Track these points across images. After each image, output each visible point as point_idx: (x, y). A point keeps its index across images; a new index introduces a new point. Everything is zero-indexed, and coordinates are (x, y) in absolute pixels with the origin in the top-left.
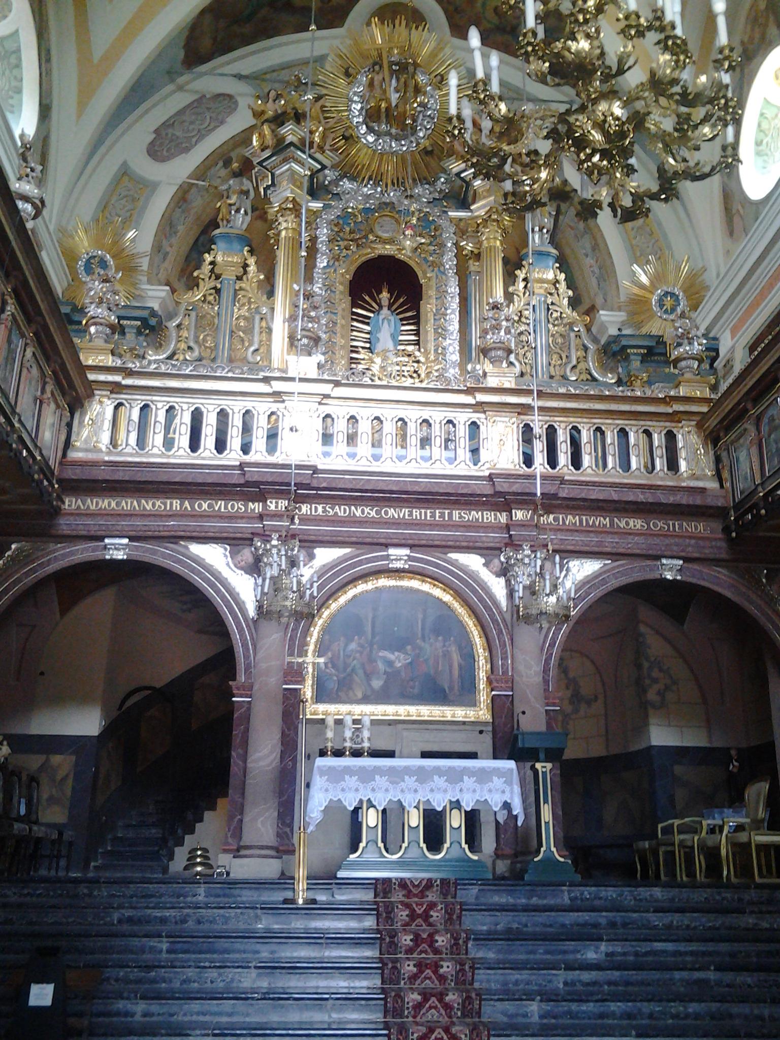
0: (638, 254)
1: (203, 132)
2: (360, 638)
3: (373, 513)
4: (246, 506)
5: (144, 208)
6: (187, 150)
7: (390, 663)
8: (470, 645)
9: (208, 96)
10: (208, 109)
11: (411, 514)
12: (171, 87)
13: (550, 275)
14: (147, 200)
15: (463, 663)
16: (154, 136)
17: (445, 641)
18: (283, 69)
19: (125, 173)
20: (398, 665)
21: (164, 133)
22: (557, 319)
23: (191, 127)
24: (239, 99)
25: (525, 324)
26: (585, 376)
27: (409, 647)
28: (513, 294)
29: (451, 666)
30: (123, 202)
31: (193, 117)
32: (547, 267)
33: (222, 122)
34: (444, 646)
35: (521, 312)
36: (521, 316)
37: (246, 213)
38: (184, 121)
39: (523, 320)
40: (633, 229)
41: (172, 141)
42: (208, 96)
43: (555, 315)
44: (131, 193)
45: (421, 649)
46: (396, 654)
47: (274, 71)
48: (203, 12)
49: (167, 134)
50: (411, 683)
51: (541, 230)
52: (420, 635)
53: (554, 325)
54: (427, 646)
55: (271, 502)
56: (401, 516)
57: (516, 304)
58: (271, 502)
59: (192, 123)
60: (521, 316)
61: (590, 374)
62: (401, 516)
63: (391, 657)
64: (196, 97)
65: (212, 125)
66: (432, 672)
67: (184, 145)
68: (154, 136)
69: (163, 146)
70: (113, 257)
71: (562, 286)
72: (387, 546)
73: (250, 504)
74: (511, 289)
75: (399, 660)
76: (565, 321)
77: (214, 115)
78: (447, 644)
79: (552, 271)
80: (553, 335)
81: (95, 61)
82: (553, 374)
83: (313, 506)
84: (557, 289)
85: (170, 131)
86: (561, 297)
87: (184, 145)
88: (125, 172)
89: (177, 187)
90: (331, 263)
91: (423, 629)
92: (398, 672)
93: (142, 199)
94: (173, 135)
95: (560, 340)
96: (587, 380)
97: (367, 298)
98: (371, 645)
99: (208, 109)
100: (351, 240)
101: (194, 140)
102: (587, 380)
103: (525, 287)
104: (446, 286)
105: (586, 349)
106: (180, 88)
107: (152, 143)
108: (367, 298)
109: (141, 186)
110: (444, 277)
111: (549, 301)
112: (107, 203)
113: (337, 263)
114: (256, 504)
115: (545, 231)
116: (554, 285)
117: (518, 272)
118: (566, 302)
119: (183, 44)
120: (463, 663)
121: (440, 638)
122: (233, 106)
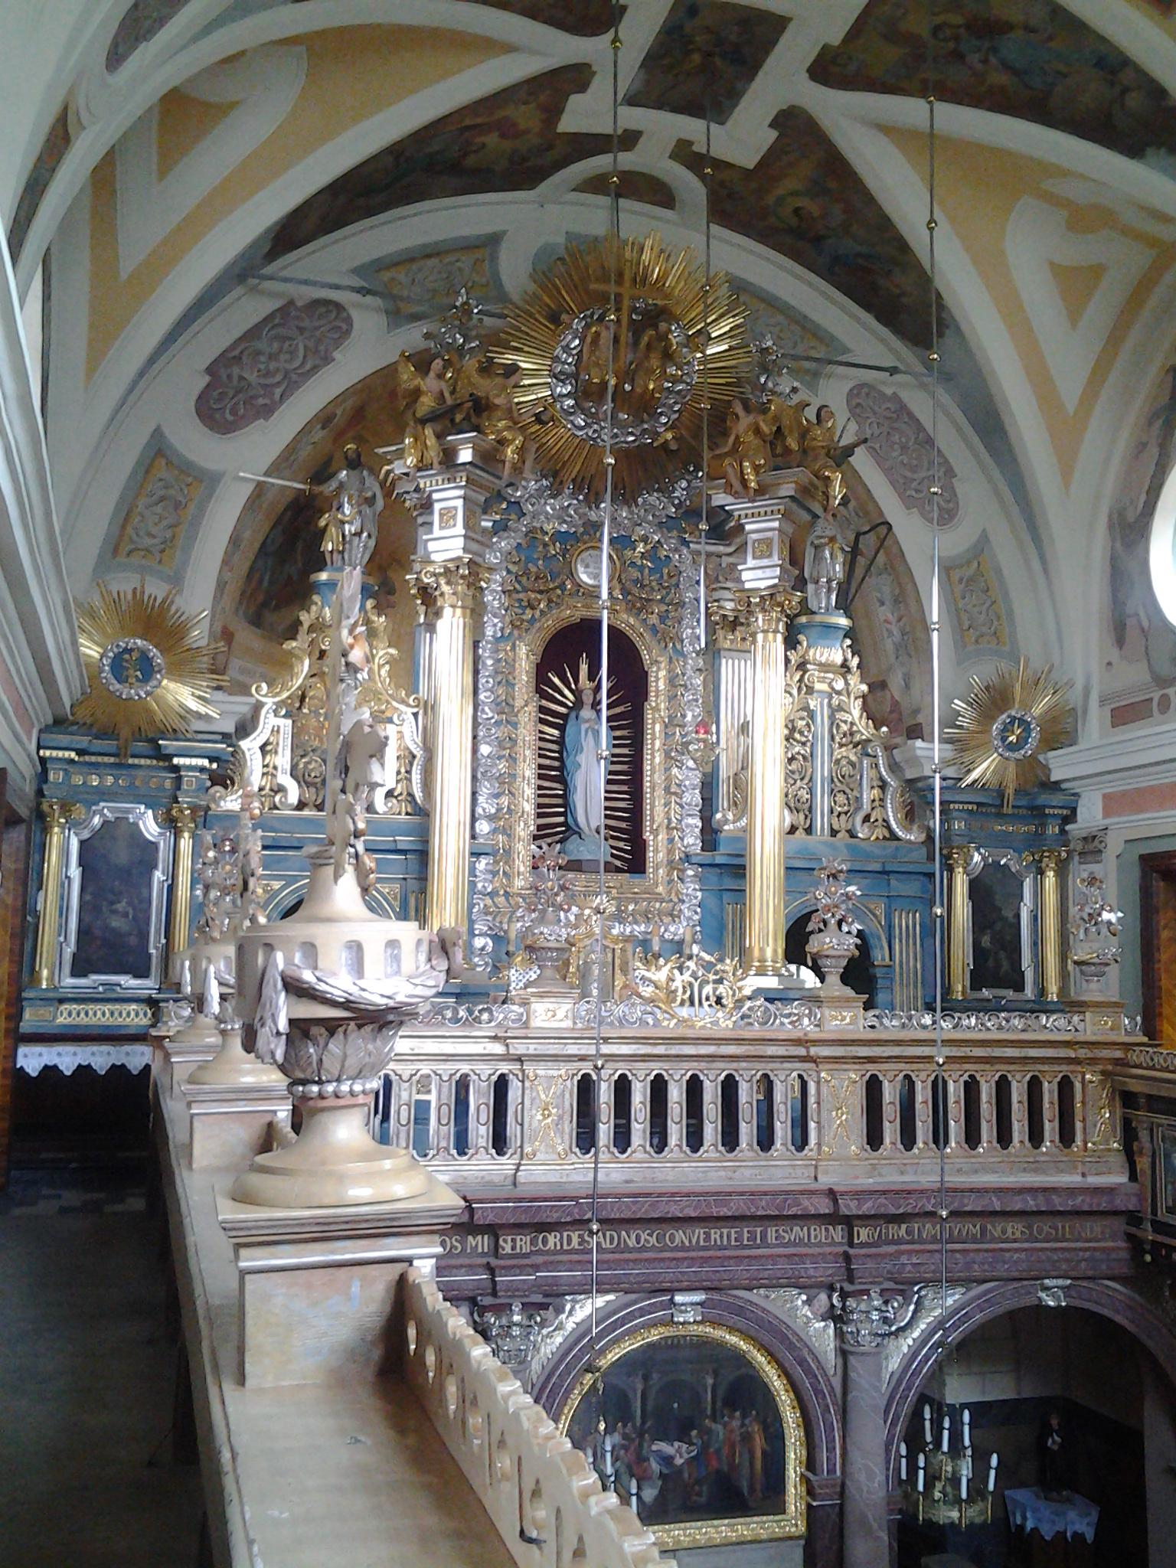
0: (966, 624)
1: (294, 377)
2: (625, 1426)
3: (653, 1240)
4: (463, 1242)
5: (196, 523)
6: (267, 411)
7: (667, 1460)
8: (779, 1419)
9: (299, 304)
10: (301, 330)
11: (708, 1236)
12: (239, 290)
15: (767, 1448)
16: (207, 378)
17: (744, 1416)
18: (428, 256)
20: (679, 1461)
21: (223, 373)
23: (273, 365)
24: (354, 314)
25: (798, 742)
26: (880, 832)
27: (694, 1433)
29: (752, 1453)
30: (159, 509)
31: (276, 345)
33: (327, 360)
34: (743, 1425)
35: (792, 721)
37: (369, 536)
38: (259, 353)
40: (961, 580)
41: (238, 392)
42: (299, 304)
43: (845, 728)
44: (172, 492)
45: (709, 1431)
46: (676, 1444)
47: (412, 260)
49: (229, 377)
50: (697, 1488)
51: (829, 581)
52: (709, 1412)
53: (841, 745)
54: (718, 1428)
55: (505, 1241)
56: (694, 1241)
58: (505, 1241)
59: (272, 357)
61: (889, 827)
62: (694, 1241)
63: (667, 1448)
64: (278, 304)
65: (308, 366)
66: (726, 1468)
67: (261, 401)
68: (207, 378)
69: (226, 402)
72: (672, 1291)
73: (470, 1238)
75: (679, 1452)
76: (857, 738)
77: (311, 344)
78: (747, 1422)
79: (840, 652)
82: (836, 827)
83: (565, 1234)
85: (236, 371)
88: (158, 451)
91: (714, 1402)
92: (679, 1471)
93: (192, 508)
94: (241, 378)
96: (884, 838)
97: (556, 680)
98: (641, 1436)
99: (301, 330)
100: (541, 592)
101: (278, 391)
102: (884, 838)
105: (883, 786)
107: (202, 399)
108: (556, 680)
109: (190, 480)
113: (516, 632)
114: (479, 1237)
120: (767, 1448)
121: (738, 1414)
122: (344, 327)
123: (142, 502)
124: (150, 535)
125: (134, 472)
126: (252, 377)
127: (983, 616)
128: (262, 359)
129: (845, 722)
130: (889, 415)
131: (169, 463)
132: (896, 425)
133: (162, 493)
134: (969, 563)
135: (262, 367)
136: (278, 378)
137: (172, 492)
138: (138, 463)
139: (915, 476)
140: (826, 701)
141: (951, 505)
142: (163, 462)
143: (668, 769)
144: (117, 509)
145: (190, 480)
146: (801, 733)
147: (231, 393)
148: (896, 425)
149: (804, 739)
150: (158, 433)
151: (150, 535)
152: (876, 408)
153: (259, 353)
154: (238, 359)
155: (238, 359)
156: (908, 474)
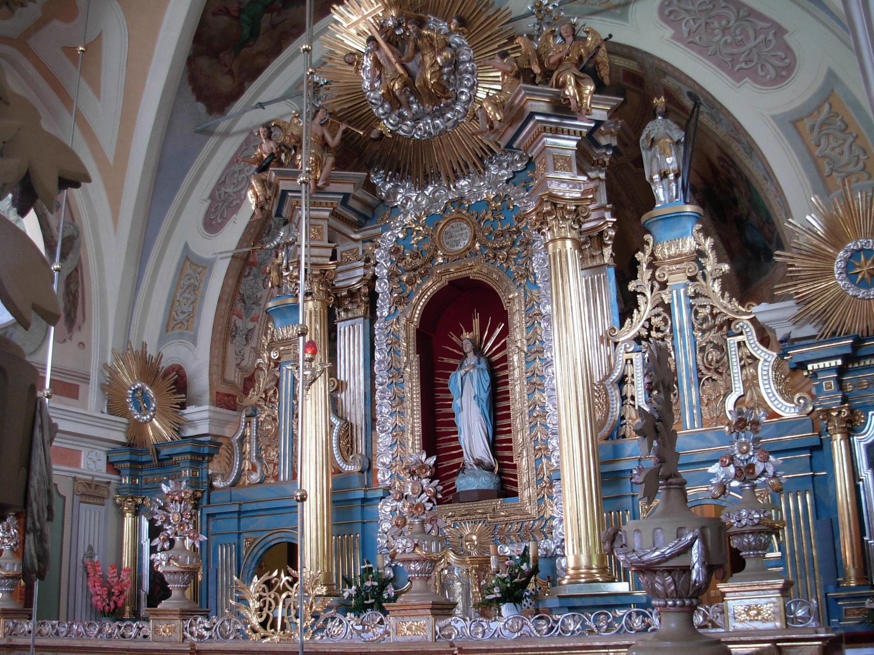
0: (827, 170)
5: (203, 297)
13: (689, 244)
14: (206, 286)
16: (209, 201)
19: (187, 258)
22: (705, 319)
28: (635, 293)
30: (186, 295)
32: (683, 236)
36: (650, 329)
38: (235, 172)
39: (653, 334)
40: (812, 128)
48: (190, 61)
51: (664, 176)
53: (704, 332)
57: (642, 308)
60: (650, 329)
64: (242, 138)
67: (235, 203)
70: (150, 387)
71: (710, 263)
74: (631, 286)
76: (719, 320)
80: (702, 349)
81: (111, 161)
84: (702, 268)
86: (709, 278)
87: (235, 203)
89: (229, 260)
90: (393, 309)
94: (225, 193)
95: (714, 355)
103: (653, 278)
104: (538, 305)
106: (226, 134)
110: (535, 291)
111: (691, 291)
112: (173, 301)
115: (671, 176)
116: (696, 261)
117: (639, 256)
118: (717, 287)
119: (194, 98)
123: (178, 294)
124: (183, 313)
125: (175, 275)
126: (230, 190)
127: (846, 153)
128: (236, 175)
129: (704, 306)
130: (704, 8)
131: (192, 263)
132: (713, 13)
133: (187, 283)
134: (819, 108)
135: (235, 181)
136: (244, 183)
137: (192, 281)
138: (177, 269)
139: (742, 49)
140: (682, 290)
141: (787, 61)
142: (188, 263)
143: (531, 394)
144: (168, 301)
145: (200, 269)
146: (658, 330)
147: (220, 204)
148: (713, 13)
149: (660, 335)
150: (186, 246)
151: (183, 313)
152: (691, 7)
153: (235, 172)
154: (224, 182)
155: (224, 182)
156: (735, 51)
